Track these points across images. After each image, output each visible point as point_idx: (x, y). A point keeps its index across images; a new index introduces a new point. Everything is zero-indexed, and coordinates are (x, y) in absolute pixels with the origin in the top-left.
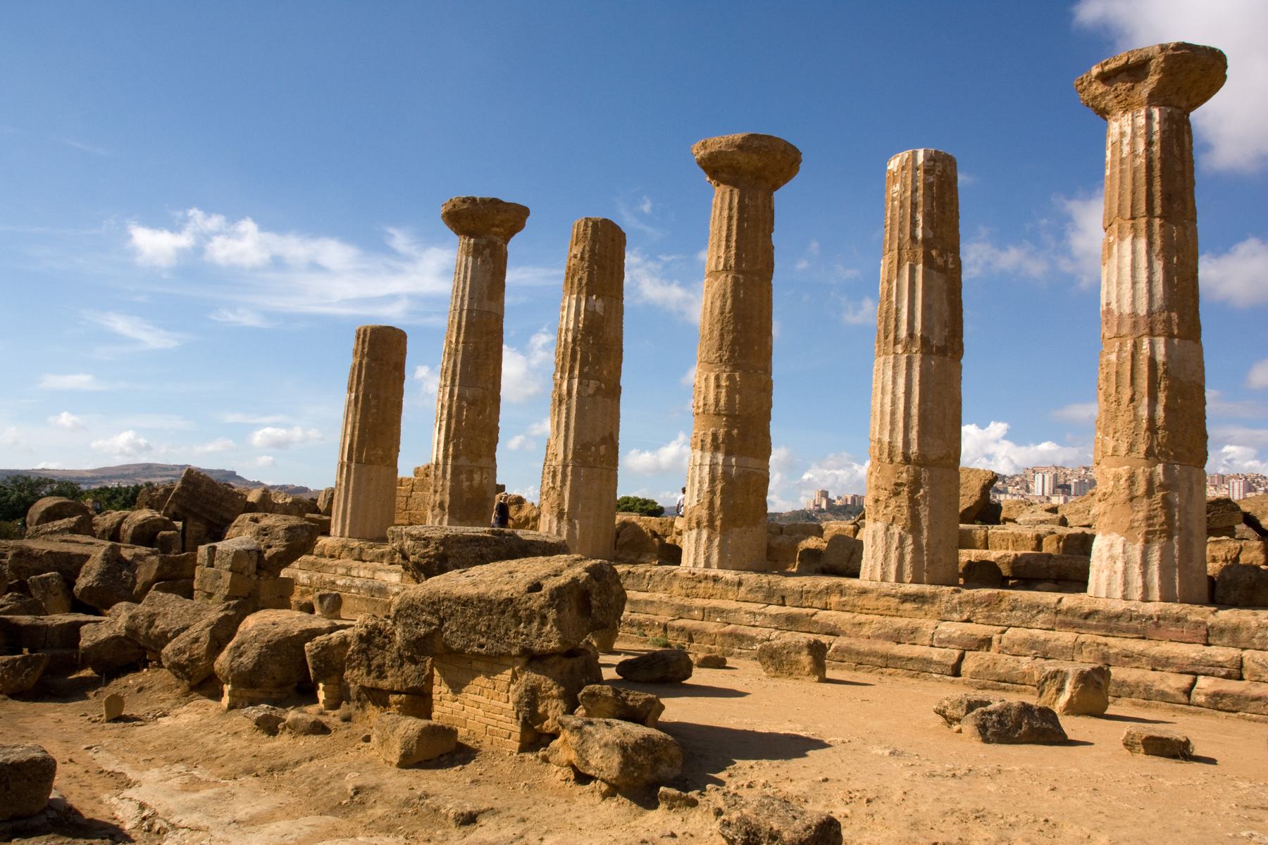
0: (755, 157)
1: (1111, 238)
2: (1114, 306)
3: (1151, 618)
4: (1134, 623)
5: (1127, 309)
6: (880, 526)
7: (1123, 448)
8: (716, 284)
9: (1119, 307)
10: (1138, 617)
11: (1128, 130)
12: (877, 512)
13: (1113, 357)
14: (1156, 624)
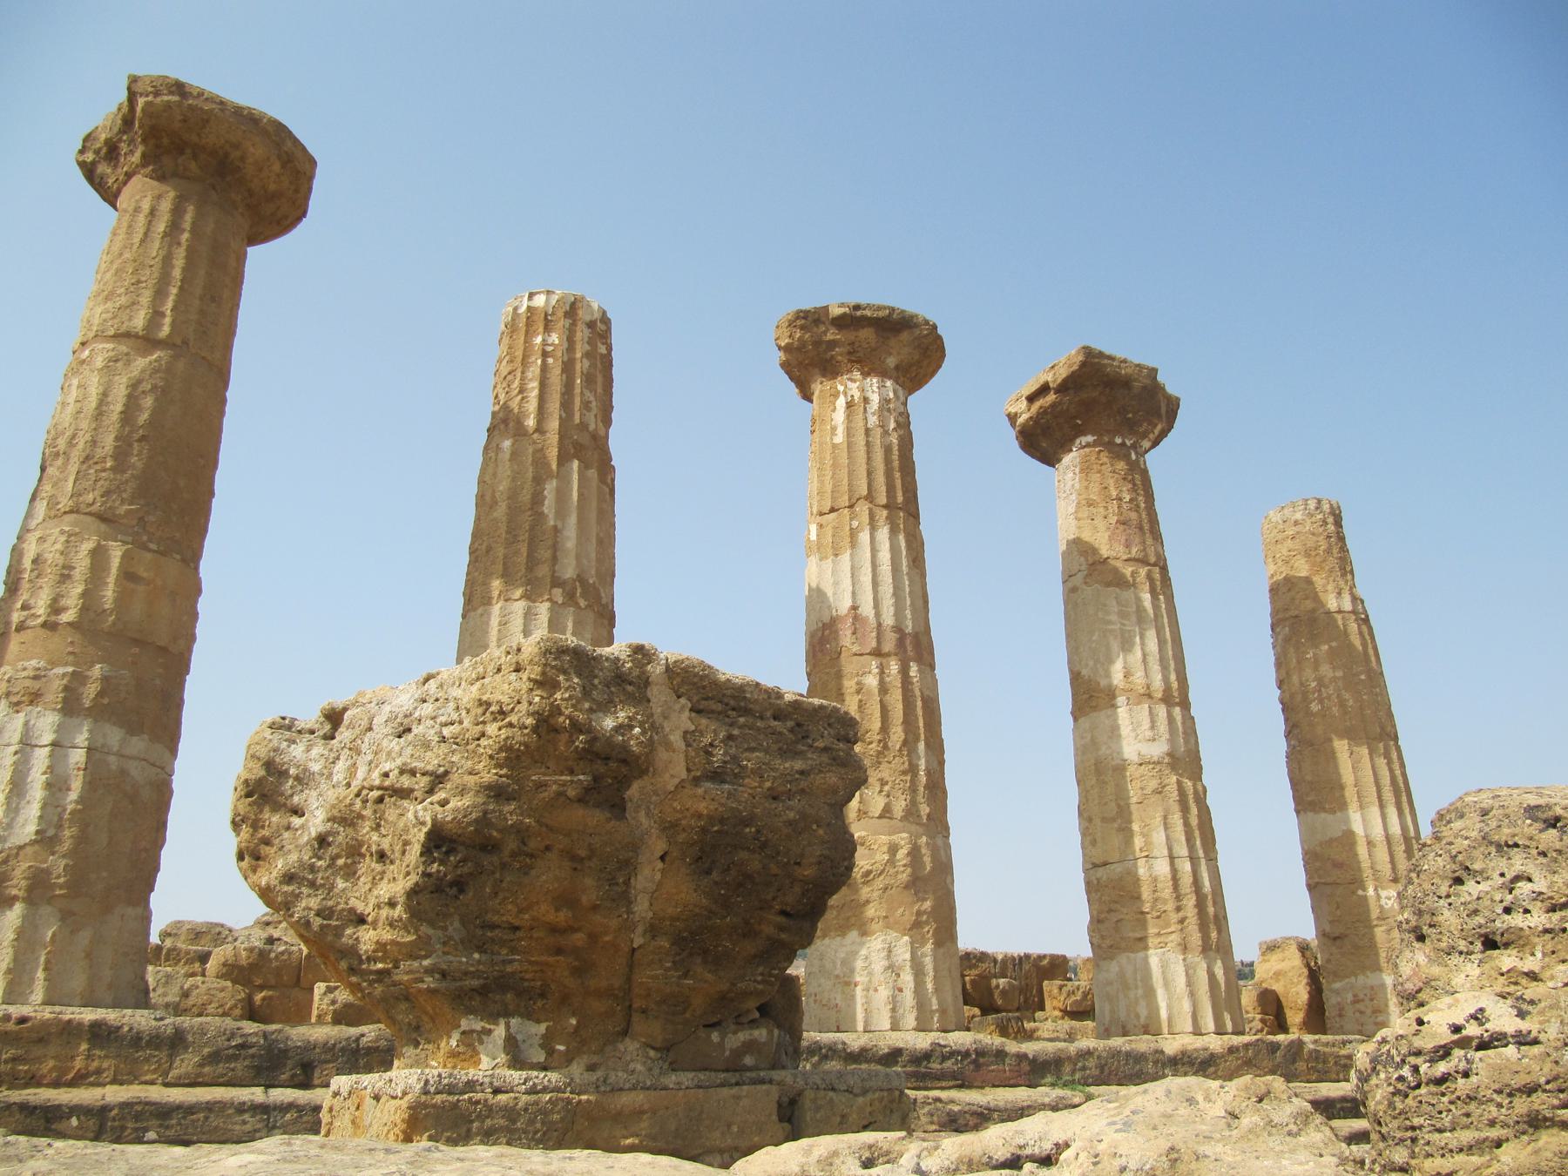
0: (277, 167)
1: (855, 524)
2: (867, 610)
3: (966, 1054)
4: (948, 1064)
5: (889, 620)
7: (899, 806)
8: (141, 363)
9: (878, 615)
10: (953, 1054)
11: (875, 398)
13: (872, 681)
14: (975, 1062)
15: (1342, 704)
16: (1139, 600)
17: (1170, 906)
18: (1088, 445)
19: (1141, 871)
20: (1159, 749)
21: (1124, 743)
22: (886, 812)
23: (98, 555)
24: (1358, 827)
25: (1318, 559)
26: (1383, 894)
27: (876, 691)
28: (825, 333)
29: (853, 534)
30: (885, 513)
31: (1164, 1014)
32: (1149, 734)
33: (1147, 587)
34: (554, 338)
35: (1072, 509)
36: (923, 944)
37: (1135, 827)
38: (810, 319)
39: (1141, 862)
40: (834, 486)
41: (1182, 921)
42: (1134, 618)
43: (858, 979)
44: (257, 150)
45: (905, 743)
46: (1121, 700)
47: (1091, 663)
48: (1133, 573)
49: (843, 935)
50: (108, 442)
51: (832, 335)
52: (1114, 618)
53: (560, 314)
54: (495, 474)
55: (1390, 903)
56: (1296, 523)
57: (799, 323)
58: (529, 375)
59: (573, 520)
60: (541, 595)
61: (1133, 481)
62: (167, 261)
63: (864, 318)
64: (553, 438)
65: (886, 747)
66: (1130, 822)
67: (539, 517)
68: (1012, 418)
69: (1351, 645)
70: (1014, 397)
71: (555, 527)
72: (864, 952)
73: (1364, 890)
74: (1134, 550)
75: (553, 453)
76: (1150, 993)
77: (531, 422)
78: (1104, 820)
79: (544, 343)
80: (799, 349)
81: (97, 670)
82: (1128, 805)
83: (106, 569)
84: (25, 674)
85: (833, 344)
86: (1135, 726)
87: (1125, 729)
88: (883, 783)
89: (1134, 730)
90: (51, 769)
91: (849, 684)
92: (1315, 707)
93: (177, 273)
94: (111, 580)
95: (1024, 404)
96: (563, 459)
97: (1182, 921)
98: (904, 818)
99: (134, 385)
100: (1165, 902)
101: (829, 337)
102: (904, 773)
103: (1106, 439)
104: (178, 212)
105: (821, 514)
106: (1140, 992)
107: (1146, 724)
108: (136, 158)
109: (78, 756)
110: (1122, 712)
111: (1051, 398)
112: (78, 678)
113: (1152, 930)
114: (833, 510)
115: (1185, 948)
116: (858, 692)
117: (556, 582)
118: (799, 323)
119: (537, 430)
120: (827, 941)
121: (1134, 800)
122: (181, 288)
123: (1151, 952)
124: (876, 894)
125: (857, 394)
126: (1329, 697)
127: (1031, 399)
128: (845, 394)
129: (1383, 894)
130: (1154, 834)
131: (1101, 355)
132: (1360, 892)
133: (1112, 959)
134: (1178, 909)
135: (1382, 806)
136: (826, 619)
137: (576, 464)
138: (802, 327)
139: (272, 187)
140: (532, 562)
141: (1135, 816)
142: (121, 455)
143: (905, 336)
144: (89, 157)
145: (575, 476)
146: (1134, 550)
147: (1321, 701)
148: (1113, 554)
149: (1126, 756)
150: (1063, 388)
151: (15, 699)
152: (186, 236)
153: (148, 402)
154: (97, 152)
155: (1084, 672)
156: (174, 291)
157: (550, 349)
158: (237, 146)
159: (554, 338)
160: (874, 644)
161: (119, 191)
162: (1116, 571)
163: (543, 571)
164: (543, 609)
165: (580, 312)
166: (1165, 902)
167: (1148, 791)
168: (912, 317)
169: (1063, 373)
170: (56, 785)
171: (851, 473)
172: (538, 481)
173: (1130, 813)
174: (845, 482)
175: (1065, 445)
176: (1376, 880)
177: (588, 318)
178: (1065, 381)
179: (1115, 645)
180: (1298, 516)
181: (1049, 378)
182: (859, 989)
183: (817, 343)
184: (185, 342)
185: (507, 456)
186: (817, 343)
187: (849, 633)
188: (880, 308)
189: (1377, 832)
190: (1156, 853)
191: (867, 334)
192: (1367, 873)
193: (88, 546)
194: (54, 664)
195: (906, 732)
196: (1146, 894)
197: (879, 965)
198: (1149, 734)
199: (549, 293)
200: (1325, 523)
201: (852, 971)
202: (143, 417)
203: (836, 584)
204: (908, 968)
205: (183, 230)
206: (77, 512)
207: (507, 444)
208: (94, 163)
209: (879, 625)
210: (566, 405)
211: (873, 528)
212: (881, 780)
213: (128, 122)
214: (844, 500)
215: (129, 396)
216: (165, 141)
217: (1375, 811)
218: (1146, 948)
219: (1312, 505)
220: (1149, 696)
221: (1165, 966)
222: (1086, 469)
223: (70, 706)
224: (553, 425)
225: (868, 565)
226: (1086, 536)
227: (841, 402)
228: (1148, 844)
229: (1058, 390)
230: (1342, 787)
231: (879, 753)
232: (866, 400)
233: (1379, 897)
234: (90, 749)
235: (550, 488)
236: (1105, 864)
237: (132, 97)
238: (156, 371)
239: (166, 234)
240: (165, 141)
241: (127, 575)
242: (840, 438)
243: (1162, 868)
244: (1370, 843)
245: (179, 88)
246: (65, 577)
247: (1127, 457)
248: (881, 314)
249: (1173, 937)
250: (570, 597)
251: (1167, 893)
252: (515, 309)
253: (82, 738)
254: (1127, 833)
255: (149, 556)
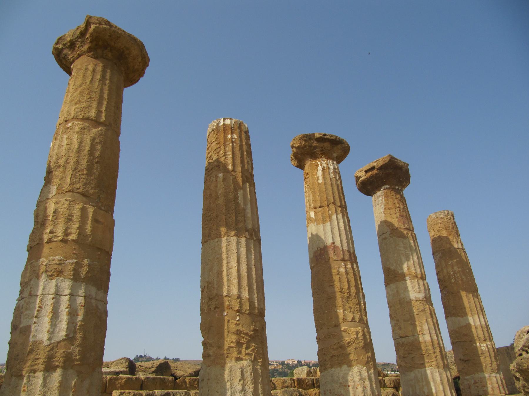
0: (140, 60)
1: (330, 212)
2: (338, 243)
5: (346, 248)
6: (246, 363)
8: (94, 131)
9: (342, 246)
11: (332, 168)
12: (240, 353)
13: (343, 270)
15: (462, 280)
16: (410, 243)
17: (432, 352)
18: (387, 189)
19: (421, 339)
20: (421, 296)
21: (410, 293)
22: (353, 320)
23: (83, 210)
24: (472, 322)
25: (450, 231)
26: (482, 345)
27: (345, 274)
28: (313, 143)
29: (330, 216)
30: (340, 209)
31: (434, 391)
32: (418, 290)
33: (412, 238)
34: (235, 136)
35: (382, 210)
36: (370, 370)
37: (417, 323)
38: (308, 138)
39: (420, 336)
40: (321, 198)
41: (436, 357)
42: (409, 249)
43: (350, 384)
44: (135, 52)
45: (356, 293)
46: (407, 278)
47: (395, 264)
48: (407, 233)
49: (341, 367)
50: (84, 162)
51: (315, 144)
52: (402, 249)
53: (236, 127)
54: (216, 187)
55: (484, 348)
56: (441, 218)
57: (304, 139)
58: (227, 149)
59: (249, 206)
60: (242, 235)
61: (402, 202)
62: (102, 90)
63: (327, 139)
64: (239, 174)
65: (350, 295)
66: (415, 321)
67: (237, 204)
68: (358, 178)
69: (463, 260)
70: (359, 170)
71: (244, 208)
72: (351, 373)
73: (476, 344)
74: (406, 225)
75: (240, 180)
76: (428, 383)
77: (230, 167)
78: (404, 321)
79: (232, 138)
80: (303, 148)
81: (86, 261)
82: (414, 315)
83: (87, 217)
84: (53, 262)
85: (315, 147)
86: (414, 287)
87: (410, 288)
88: (351, 308)
89: (413, 289)
90: (70, 306)
91: (334, 271)
92: (453, 281)
93: (106, 96)
94: (89, 222)
95: (364, 173)
96: (244, 182)
97: (436, 357)
98: (359, 322)
99: (93, 140)
100: (430, 350)
101: (314, 144)
102: (357, 304)
103: (393, 187)
104: (104, 72)
105: (315, 208)
106: (424, 383)
107: (417, 287)
108: (86, 47)
109: (81, 300)
110: (408, 282)
111: (375, 171)
112: (78, 265)
113: (426, 361)
114: (320, 207)
115: (438, 367)
116: (338, 274)
117: (247, 230)
118: (304, 139)
119: (233, 171)
120: (333, 369)
121: (415, 314)
122: (107, 102)
123: (427, 368)
124: (352, 351)
125: (325, 166)
126: (458, 277)
127: (366, 172)
128: (321, 165)
129: (482, 345)
130: (424, 326)
131: (394, 158)
132: (474, 345)
133: (411, 371)
134: (434, 353)
135: (478, 315)
136: (322, 246)
137: (248, 185)
138: (305, 140)
139: (136, 67)
140: (237, 222)
141: (416, 319)
142: (90, 168)
143: (339, 146)
144: (60, 46)
145: (248, 189)
146: (406, 225)
147: (455, 279)
148: (399, 226)
149: (411, 298)
150: (380, 168)
151: (50, 274)
152: (107, 82)
153: (99, 147)
154: (64, 45)
155: (392, 268)
156: (105, 103)
157: (234, 140)
158: (128, 49)
159: (235, 136)
160: (342, 256)
161: (73, 61)
162: (401, 232)
163: (241, 225)
164: (243, 240)
165: (243, 128)
166: (430, 350)
167: (420, 310)
168: (342, 140)
169: (381, 163)
170: (73, 313)
171: (327, 194)
172: (236, 190)
173: (415, 318)
174: (325, 196)
175: (378, 188)
176: (479, 340)
177: (245, 130)
178: (382, 166)
179: (403, 258)
180: (442, 216)
181: (375, 165)
182: (350, 388)
183: (310, 146)
184: (110, 125)
185: (221, 180)
186: (310, 146)
187: (332, 252)
188: (332, 136)
189: (478, 324)
190: (425, 332)
191: (327, 145)
192: (476, 338)
193: (79, 207)
194: (67, 258)
195: (356, 289)
196: (423, 347)
197: (357, 379)
198: (418, 290)
199: (231, 119)
200: (450, 219)
201: (347, 381)
202: (98, 153)
203: (325, 234)
204: (367, 379)
205: (107, 79)
206: (73, 192)
207: (221, 175)
208: (62, 49)
209: (343, 249)
210: (242, 162)
211: (337, 214)
212: (350, 307)
213: (83, 34)
214: (326, 203)
215: (92, 144)
216: (100, 43)
217: (476, 316)
218: (425, 367)
219: (446, 213)
220: (417, 276)
221: (432, 373)
222: (386, 197)
223: (76, 278)
224: (239, 169)
225: (337, 227)
226: (389, 220)
227: (320, 168)
228: (422, 330)
229: (378, 169)
230: (465, 308)
231: (348, 297)
232: (329, 168)
233: (481, 346)
234: (85, 297)
235: (240, 193)
236: (406, 337)
237: (88, 24)
238: (100, 135)
239: (100, 80)
240: (100, 43)
241: (95, 220)
242: (321, 181)
243: (427, 338)
244: (476, 328)
245: (108, 23)
246: (69, 219)
247: (400, 193)
248: (333, 138)
249: (434, 363)
250: (251, 235)
251: (430, 347)
252: (218, 124)
253: (82, 292)
254: (415, 326)
255: (102, 212)
